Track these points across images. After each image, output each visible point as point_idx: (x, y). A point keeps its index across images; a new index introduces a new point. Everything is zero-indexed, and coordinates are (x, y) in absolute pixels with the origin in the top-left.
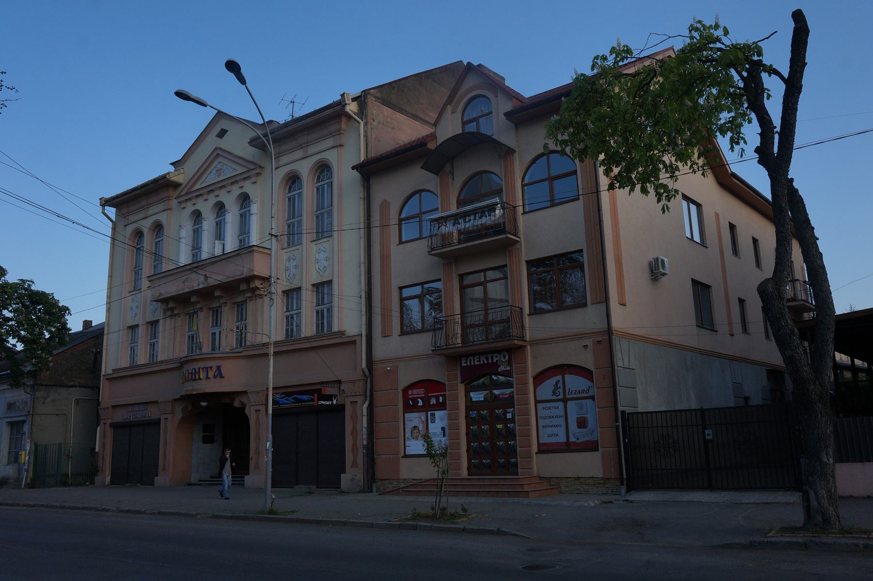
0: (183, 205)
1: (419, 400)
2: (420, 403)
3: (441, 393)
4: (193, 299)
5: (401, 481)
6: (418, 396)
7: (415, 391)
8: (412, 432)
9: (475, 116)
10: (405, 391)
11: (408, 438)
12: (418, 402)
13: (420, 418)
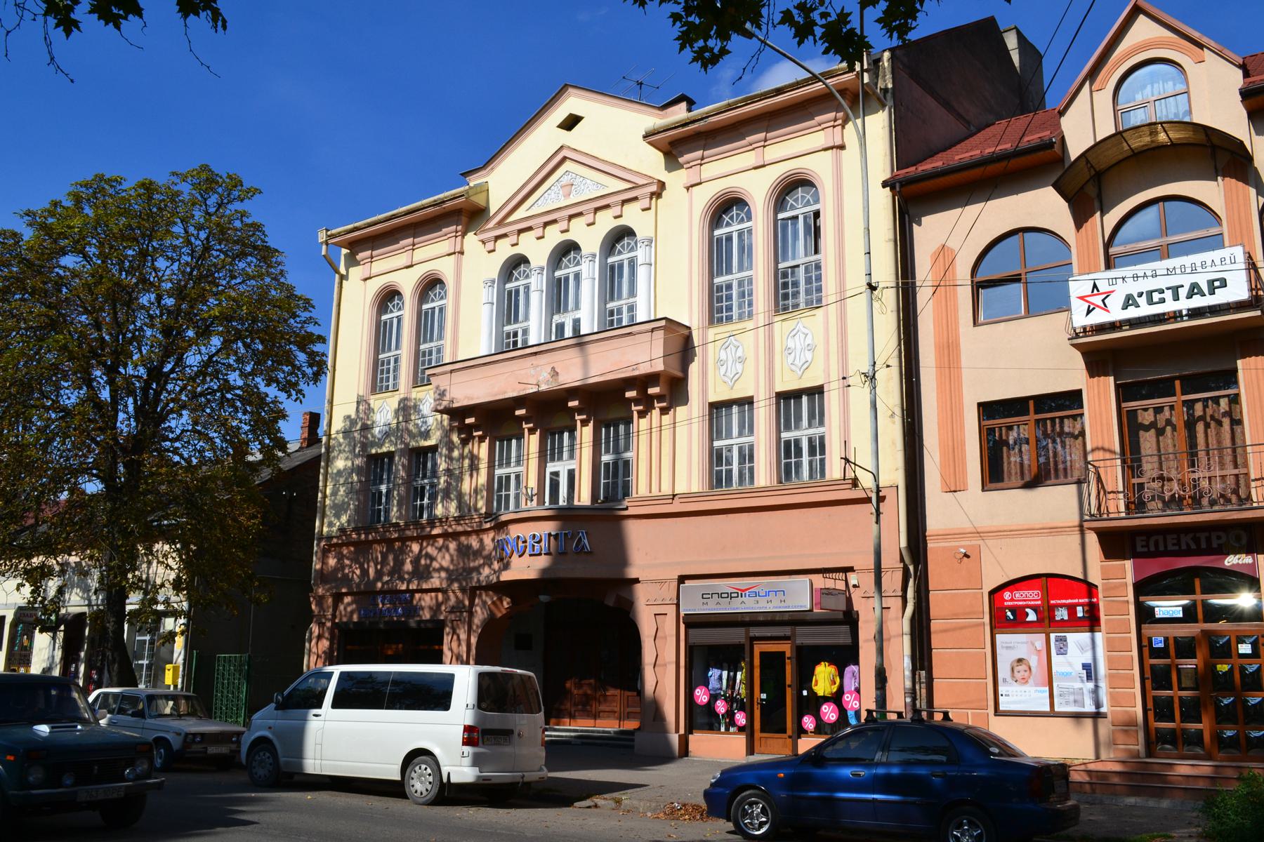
0: (490, 246)
1: (1028, 610)
2: (1032, 616)
3: (1080, 601)
4: (573, 404)
6: (1025, 603)
7: (1018, 595)
8: (1013, 670)
10: (995, 592)
11: (1005, 680)
12: (1027, 615)
13: (1033, 644)
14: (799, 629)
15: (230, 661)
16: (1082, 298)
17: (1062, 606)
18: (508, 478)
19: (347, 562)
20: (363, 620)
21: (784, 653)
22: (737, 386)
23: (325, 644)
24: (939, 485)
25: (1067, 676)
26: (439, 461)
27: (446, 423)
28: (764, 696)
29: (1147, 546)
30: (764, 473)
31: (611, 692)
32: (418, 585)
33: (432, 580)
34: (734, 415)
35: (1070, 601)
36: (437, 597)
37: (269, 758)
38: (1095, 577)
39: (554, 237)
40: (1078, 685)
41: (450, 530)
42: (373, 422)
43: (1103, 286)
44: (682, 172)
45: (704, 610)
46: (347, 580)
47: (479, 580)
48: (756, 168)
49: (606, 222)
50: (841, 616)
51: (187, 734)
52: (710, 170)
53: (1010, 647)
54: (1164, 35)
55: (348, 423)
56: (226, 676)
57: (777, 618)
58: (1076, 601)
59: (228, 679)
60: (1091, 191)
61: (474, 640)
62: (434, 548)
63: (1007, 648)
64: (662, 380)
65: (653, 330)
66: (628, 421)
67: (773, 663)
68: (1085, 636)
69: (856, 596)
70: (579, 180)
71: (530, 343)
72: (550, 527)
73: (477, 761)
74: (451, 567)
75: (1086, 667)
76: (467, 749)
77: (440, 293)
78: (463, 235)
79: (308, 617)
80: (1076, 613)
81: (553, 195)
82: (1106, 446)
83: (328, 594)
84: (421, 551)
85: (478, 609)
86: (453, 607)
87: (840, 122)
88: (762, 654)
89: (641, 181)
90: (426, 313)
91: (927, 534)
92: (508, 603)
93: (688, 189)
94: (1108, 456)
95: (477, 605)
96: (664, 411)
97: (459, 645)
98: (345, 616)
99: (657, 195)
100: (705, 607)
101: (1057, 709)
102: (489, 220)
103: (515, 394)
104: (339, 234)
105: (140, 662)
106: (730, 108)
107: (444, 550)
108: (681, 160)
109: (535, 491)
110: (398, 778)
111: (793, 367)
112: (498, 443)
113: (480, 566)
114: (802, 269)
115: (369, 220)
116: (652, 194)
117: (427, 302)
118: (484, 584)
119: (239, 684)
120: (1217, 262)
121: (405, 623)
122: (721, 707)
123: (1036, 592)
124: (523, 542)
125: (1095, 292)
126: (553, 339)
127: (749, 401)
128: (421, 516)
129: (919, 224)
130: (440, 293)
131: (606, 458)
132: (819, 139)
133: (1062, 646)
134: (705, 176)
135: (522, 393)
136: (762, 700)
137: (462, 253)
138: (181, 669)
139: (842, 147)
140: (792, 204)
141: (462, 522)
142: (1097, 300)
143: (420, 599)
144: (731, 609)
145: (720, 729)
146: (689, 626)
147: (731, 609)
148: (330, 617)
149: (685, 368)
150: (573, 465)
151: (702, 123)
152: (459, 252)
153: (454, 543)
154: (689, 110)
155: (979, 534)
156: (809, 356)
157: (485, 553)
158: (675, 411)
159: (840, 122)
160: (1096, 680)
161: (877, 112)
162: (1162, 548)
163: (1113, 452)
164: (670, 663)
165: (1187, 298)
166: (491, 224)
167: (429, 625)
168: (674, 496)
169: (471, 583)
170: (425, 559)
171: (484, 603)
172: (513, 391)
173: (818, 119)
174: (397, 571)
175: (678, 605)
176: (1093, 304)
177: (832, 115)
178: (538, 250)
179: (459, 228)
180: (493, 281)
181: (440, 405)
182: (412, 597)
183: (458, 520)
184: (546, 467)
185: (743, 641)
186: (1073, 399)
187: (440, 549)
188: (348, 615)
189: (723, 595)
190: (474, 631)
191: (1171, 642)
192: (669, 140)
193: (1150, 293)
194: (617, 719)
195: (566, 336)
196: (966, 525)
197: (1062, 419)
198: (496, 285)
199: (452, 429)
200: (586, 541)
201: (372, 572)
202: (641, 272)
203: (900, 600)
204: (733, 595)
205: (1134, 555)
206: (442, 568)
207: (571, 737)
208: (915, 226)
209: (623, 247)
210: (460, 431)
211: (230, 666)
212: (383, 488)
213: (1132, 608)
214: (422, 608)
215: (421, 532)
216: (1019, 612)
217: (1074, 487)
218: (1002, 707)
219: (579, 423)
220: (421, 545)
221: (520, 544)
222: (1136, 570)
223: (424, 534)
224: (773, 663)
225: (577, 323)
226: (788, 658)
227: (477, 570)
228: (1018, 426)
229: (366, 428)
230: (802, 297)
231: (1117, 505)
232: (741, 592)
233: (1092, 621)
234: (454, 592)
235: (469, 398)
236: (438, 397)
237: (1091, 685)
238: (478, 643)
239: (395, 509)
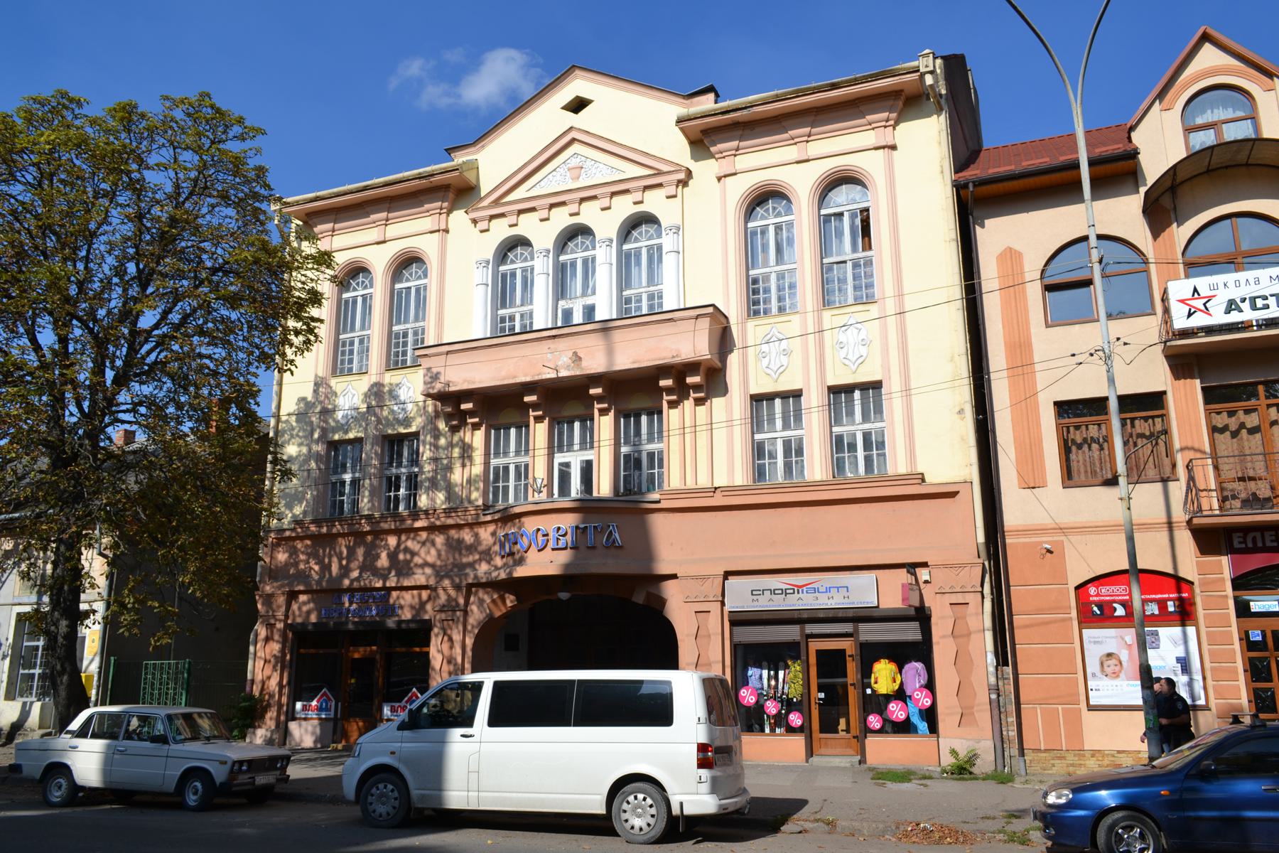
1: (1115, 605)
2: (1120, 611)
3: (1171, 596)
5: (1088, 755)
7: (1104, 590)
8: (1102, 664)
9: (1216, 119)
11: (1094, 675)
12: (1115, 609)
13: (1123, 639)
15: (162, 668)
16: (1182, 301)
17: (1152, 601)
18: (506, 469)
19: (302, 557)
20: (324, 620)
21: (844, 651)
23: (275, 647)
24: (1016, 481)
26: (421, 449)
27: (430, 409)
28: (822, 695)
29: (1245, 542)
30: (816, 466)
33: (416, 576)
34: (856, 402)
36: (420, 596)
37: (392, 791)
39: (562, 219)
41: (438, 523)
42: (335, 406)
43: (1204, 291)
44: (711, 162)
45: (754, 607)
46: (303, 576)
47: (476, 577)
48: (798, 162)
49: (624, 208)
50: (912, 612)
51: (234, 762)
52: (743, 161)
53: (1098, 642)
54: (1230, 63)
55: (302, 405)
56: (157, 685)
58: (1166, 596)
59: (160, 689)
60: (1166, 201)
61: (469, 642)
62: (415, 542)
63: (1095, 642)
64: (702, 369)
65: (697, 317)
67: (831, 663)
68: (1177, 631)
69: (927, 592)
70: (589, 163)
71: (535, 328)
72: (568, 521)
73: (715, 788)
74: (439, 563)
75: (1178, 660)
76: (704, 773)
77: (416, 272)
78: (449, 212)
79: (253, 616)
80: (1166, 607)
81: (558, 177)
82: (1196, 446)
83: (279, 592)
84: (398, 545)
86: (444, 606)
87: (892, 122)
88: (820, 653)
89: (665, 168)
90: (400, 293)
91: (1005, 529)
92: (511, 602)
93: (719, 179)
94: (1199, 455)
95: (473, 603)
96: (699, 402)
97: (451, 647)
98: (300, 616)
99: (684, 183)
100: (756, 603)
102: (481, 199)
103: (528, 379)
104: (297, 203)
105: (32, 671)
106: (777, 99)
107: (428, 544)
108: (713, 149)
109: (545, 482)
110: (601, 810)
111: (847, 362)
112: (493, 431)
113: (475, 562)
114: (849, 264)
115: (335, 190)
116: (679, 181)
117: (401, 281)
118: (484, 580)
119: (175, 694)
120: (1252, 281)
121: (382, 623)
122: (772, 708)
123: (1123, 587)
124: (544, 536)
125: (1196, 295)
127: (797, 394)
128: (397, 507)
129: (983, 226)
130: (416, 272)
131: (624, 450)
132: (869, 138)
133: (1153, 640)
134: (739, 167)
135: (537, 378)
136: (820, 699)
137: (447, 231)
138: (96, 678)
139: (893, 148)
141: (453, 514)
142: (1199, 304)
144: (786, 605)
145: (762, 730)
146: (734, 623)
147: (786, 605)
148: (283, 618)
149: (723, 359)
150: (589, 455)
151: (745, 112)
152: (443, 230)
154: (716, 102)
155: (1061, 530)
156: (863, 351)
157: (480, 548)
158: (711, 402)
159: (892, 122)
161: (929, 116)
162: (1260, 544)
163: (1204, 452)
165: (1226, 313)
166: (485, 203)
167: (413, 626)
168: (716, 488)
169: (466, 580)
170: (405, 554)
171: (481, 601)
172: (525, 375)
174: (369, 566)
175: (723, 604)
176: (1194, 307)
177: (885, 115)
178: (542, 232)
179: (445, 204)
180: (488, 262)
181: (433, 388)
182: (389, 595)
183: (448, 512)
184: (553, 458)
185: (798, 638)
186: (1152, 402)
187: (424, 544)
188: (304, 615)
189: (776, 592)
190: (470, 632)
191: (1269, 635)
192: (703, 128)
193: (1253, 300)
195: (575, 322)
196: (1045, 520)
197: (1133, 420)
198: (490, 266)
199: (437, 414)
200: (617, 535)
201: (335, 569)
202: (669, 262)
203: (719, 604)
204: (788, 591)
205: (1231, 550)
206: (426, 564)
208: (977, 228)
209: (516, 256)
210: (449, 417)
211: (162, 674)
212: (348, 477)
213: (1231, 603)
214: (401, 607)
215: (400, 525)
217: (1159, 486)
218: (1092, 703)
219: (532, 419)
220: (399, 538)
221: (540, 538)
222: (1234, 565)
223: (403, 527)
224: (831, 663)
225: (590, 311)
226: (849, 656)
227: (471, 565)
228: (1087, 426)
229: (326, 412)
230: (774, 305)
231: (1211, 503)
233: (1185, 615)
234: (444, 589)
235: (469, 382)
236: (430, 380)
239: (366, 500)
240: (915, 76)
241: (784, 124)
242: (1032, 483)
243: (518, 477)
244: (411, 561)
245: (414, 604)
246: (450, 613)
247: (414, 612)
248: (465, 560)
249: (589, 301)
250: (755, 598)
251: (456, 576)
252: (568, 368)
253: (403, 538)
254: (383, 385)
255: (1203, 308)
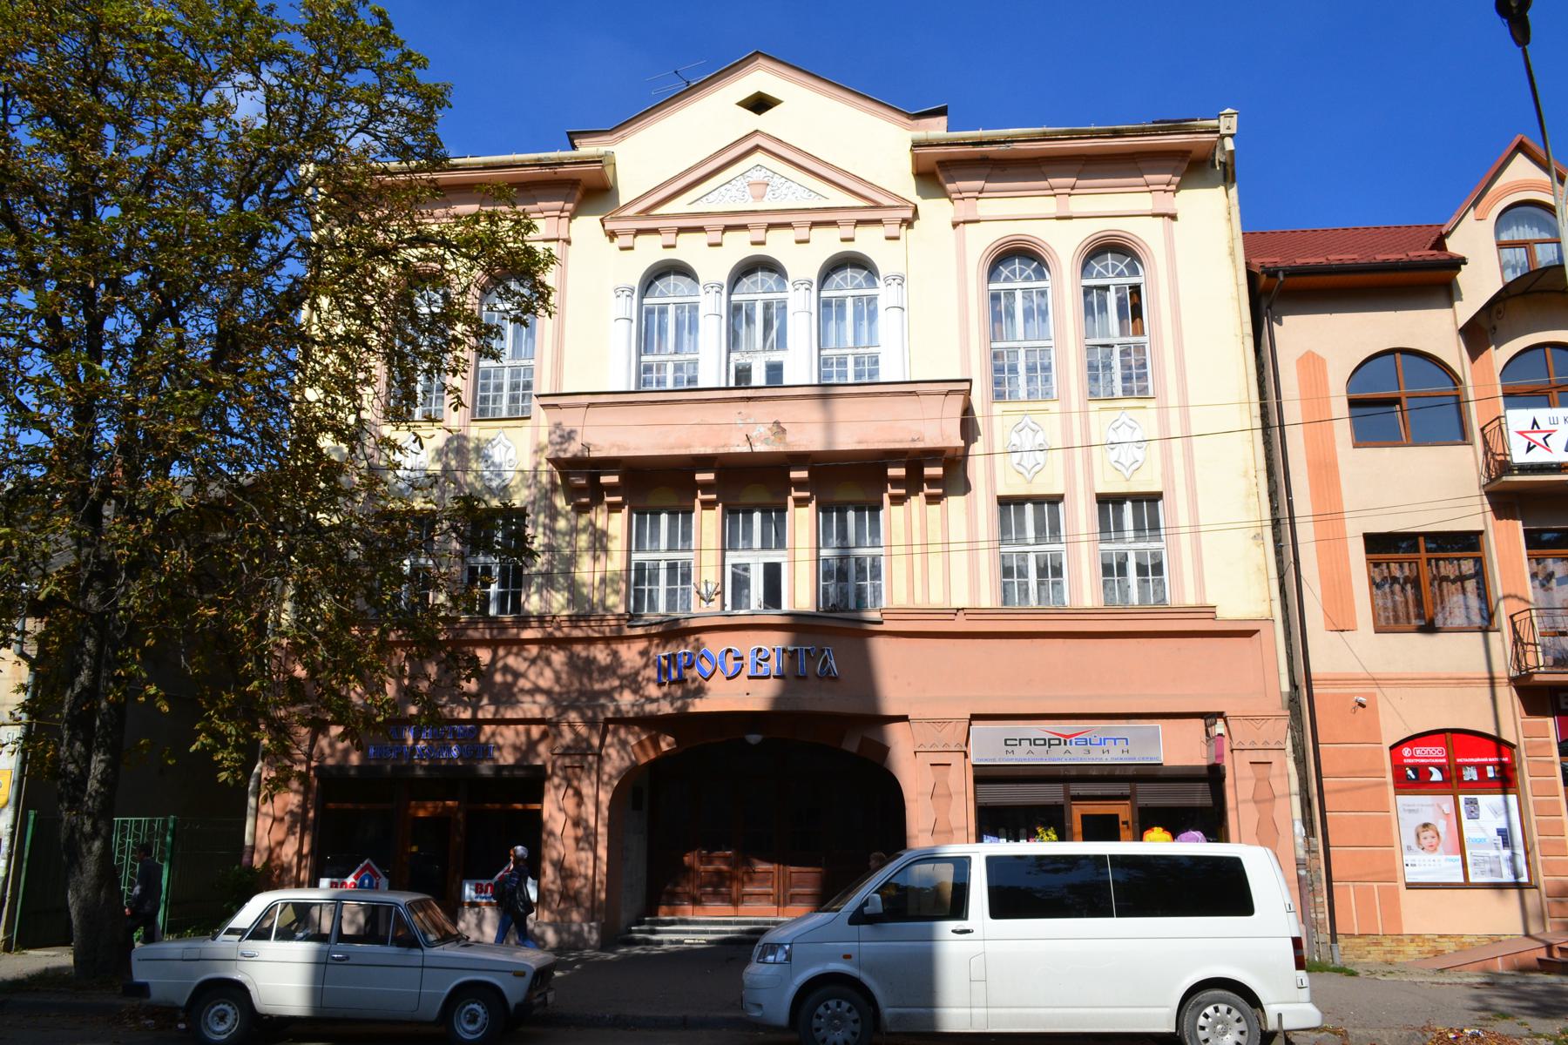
1: (1431, 769)
2: (1437, 776)
5: (1407, 940)
7: (1419, 751)
8: (1418, 836)
9: (1529, 237)
10: (1395, 748)
11: (1409, 848)
12: (1431, 774)
13: (1439, 807)
14: (1141, 787)
16: (1521, 433)
17: (1470, 765)
21: (1116, 817)
22: (1038, 479)
23: (290, 800)
25: (1480, 843)
26: (529, 531)
31: (762, 867)
32: (497, 711)
33: (525, 706)
35: (1478, 760)
36: (528, 733)
38: (1508, 735)
39: (739, 247)
40: (1493, 853)
41: (558, 634)
43: (1544, 425)
47: (618, 709)
48: (1058, 218)
49: (828, 244)
52: (986, 207)
57: (1117, 773)
58: (1485, 760)
61: (605, 797)
63: (1410, 811)
65: (948, 393)
66: (876, 508)
68: (1498, 798)
70: (777, 180)
74: (557, 689)
75: (1500, 832)
80: (1486, 772)
81: (734, 192)
82: (1520, 594)
84: (494, 661)
85: (613, 752)
86: (568, 747)
88: (1084, 817)
89: (886, 201)
92: (669, 745)
93: (955, 225)
96: (932, 500)
97: (580, 804)
98: (332, 755)
99: (908, 223)
100: (1010, 756)
101: (1472, 880)
103: (709, 451)
106: (1045, 138)
107: (540, 663)
108: (950, 187)
110: (1170, 1028)
113: (613, 689)
114: (1117, 350)
116: (904, 220)
118: (631, 715)
123: (1439, 749)
124: (735, 659)
126: (732, 383)
135: (721, 451)
139: (1173, 217)
140: (757, 281)
141: (583, 624)
142: (1538, 438)
143: (493, 734)
146: (978, 780)
151: (1003, 147)
152: (564, 240)
153: (562, 653)
155: (1375, 681)
157: (621, 672)
159: (1173, 187)
160: (1513, 847)
161: (1215, 186)
163: (1528, 602)
164: (958, 829)
166: (631, 211)
167: (519, 773)
170: (504, 674)
172: (704, 445)
173: (1054, 181)
179: (570, 206)
181: (565, 451)
182: (479, 730)
183: (574, 620)
185: (1060, 800)
186: (1469, 541)
188: (338, 755)
190: (606, 784)
192: (938, 159)
194: (774, 903)
195: (753, 383)
197: (1437, 560)
199: (554, 488)
200: (833, 662)
206: (536, 690)
207: (742, 932)
210: (572, 493)
214: (499, 748)
215: (499, 634)
216: (1422, 771)
217: (1479, 636)
220: (495, 653)
223: (504, 637)
225: (775, 371)
226: (1124, 823)
228: (1388, 564)
232: (1064, 739)
233: (1505, 781)
234: (571, 725)
236: (559, 440)
237: (1507, 853)
238: (612, 801)
240: (1212, 137)
241: (1044, 169)
242: (1341, 627)
243: (671, 579)
244: (514, 683)
245: (518, 743)
246: (578, 757)
247: (518, 755)
248: (597, 686)
249: (776, 357)
250: (1010, 748)
251: (588, 707)
252: (766, 441)
253: (501, 652)
254: (465, 438)
255: (1543, 443)
